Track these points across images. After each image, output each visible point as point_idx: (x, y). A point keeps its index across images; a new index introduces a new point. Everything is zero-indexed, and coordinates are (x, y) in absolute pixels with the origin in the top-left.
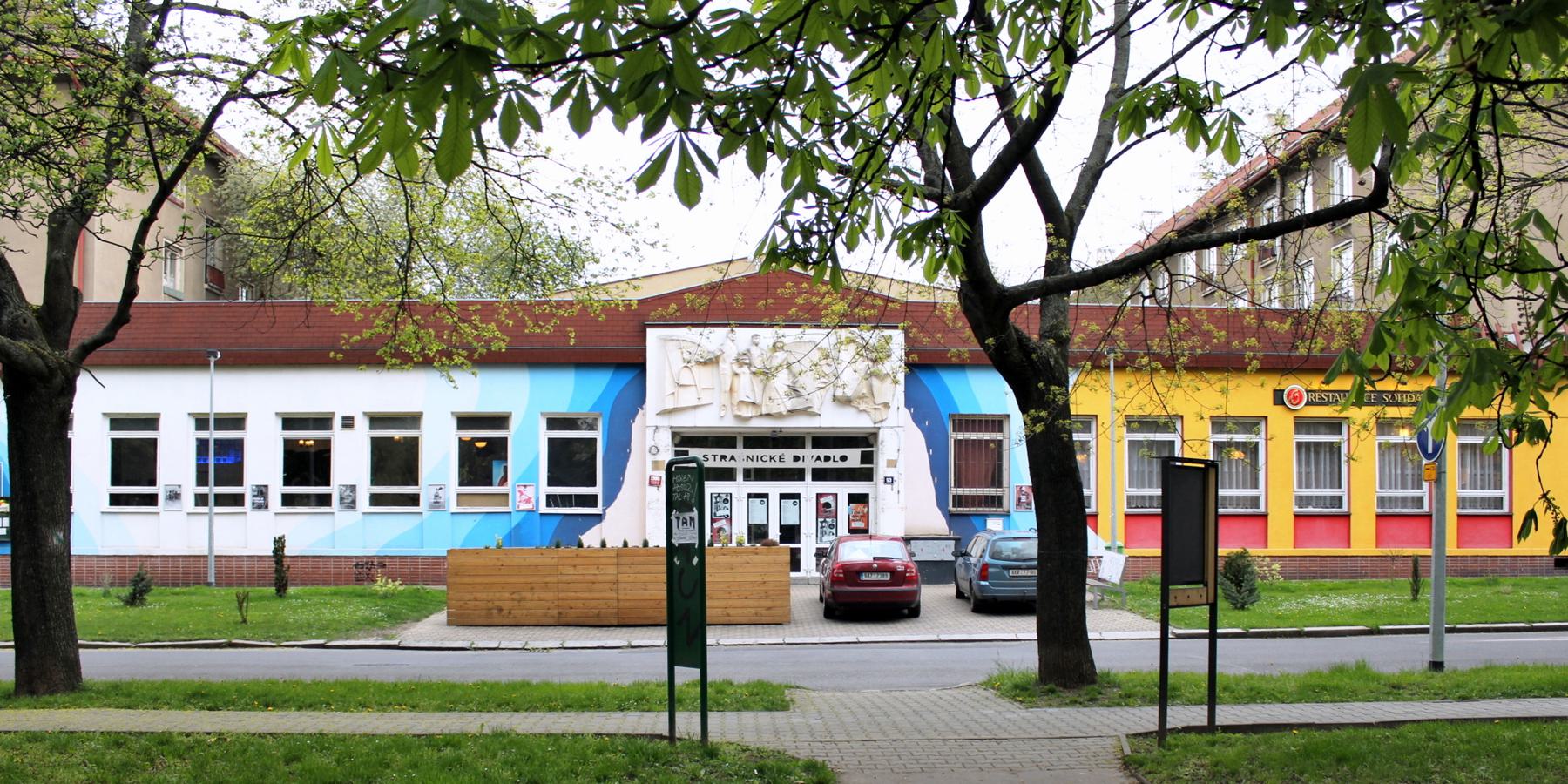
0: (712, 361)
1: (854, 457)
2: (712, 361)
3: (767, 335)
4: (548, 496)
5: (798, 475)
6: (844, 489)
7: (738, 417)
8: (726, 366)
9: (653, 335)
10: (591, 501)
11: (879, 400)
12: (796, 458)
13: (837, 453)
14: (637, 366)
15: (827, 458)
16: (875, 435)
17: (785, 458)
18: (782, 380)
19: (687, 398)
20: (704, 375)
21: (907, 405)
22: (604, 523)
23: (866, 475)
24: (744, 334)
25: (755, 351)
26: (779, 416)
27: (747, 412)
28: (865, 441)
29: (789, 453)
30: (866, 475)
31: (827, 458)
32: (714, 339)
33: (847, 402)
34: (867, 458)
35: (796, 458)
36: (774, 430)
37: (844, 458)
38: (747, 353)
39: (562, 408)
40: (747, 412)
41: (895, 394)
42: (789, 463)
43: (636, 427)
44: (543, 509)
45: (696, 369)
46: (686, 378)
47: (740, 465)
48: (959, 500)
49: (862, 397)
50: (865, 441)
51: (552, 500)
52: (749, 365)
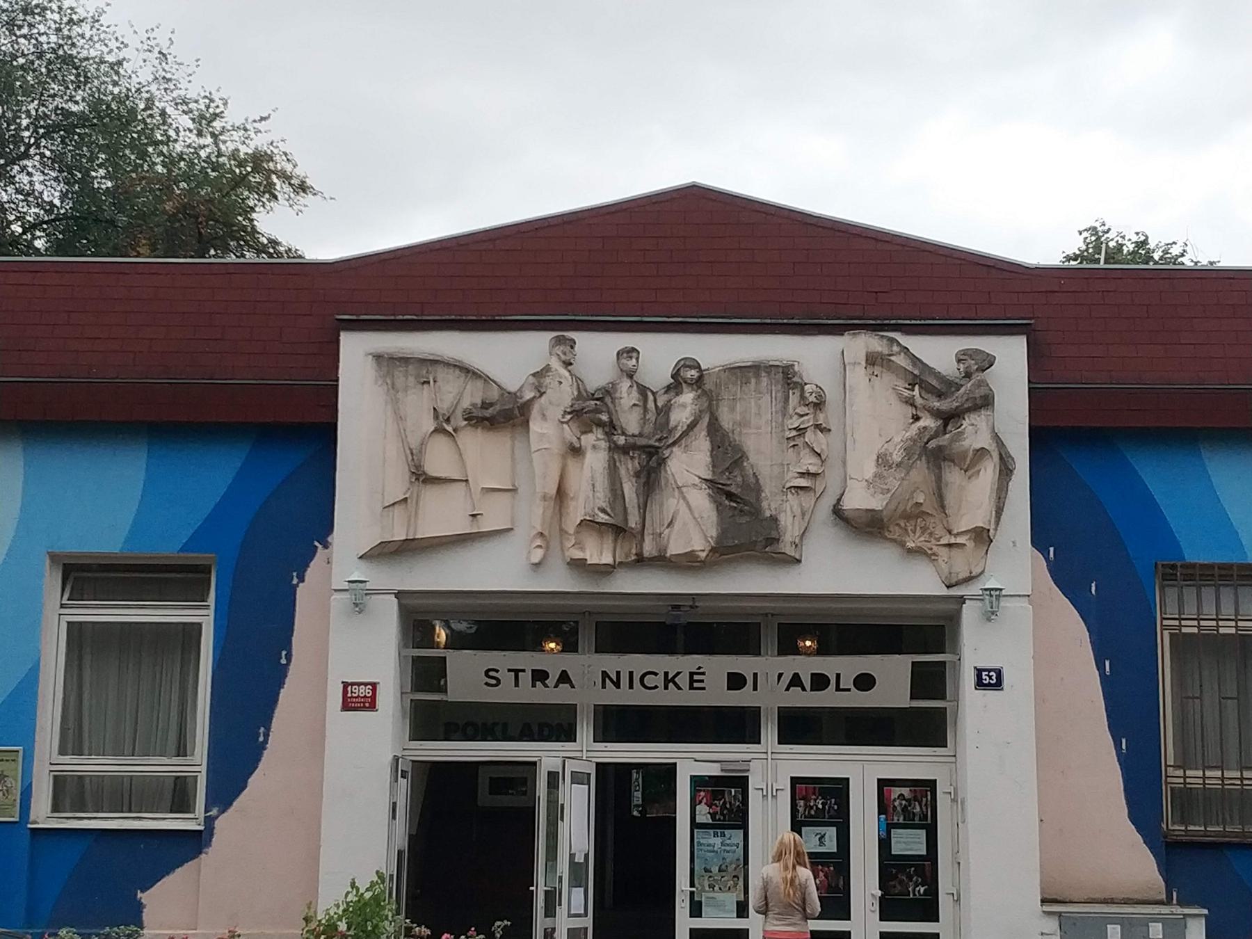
0: (504, 415)
1: (892, 681)
2: (504, 415)
3: (660, 353)
4: (59, 783)
5: (737, 725)
6: (863, 769)
7: (578, 565)
8: (547, 429)
9: (356, 352)
10: (178, 795)
11: (965, 524)
12: (736, 681)
13: (846, 666)
14: (310, 433)
15: (820, 682)
16: (954, 619)
17: (708, 679)
18: (689, 465)
19: (441, 514)
20: (484, 454)
21: (1039, 541)
22: (207, 859)
23: (927, 728)
24: (597, 352)
25: (627, 396)
26: (688, 564)
27: (598, 552)
28: (922, 635)
29: (716, 667)
30: (927, 728)
31: (820, 682)
32: (509, 357)
33: (867, 527)
34: (931, 681)
35: (736, 681)
36: (675, 602)
37: (865, 682)
38: (606, 394)
39: (107, 532)
40: (598, 552)
41: (996, 502)
42: (716, 695)
43: (304, 595)
44: (42, 815)
45: (474, 442)
46: (439, 460)
47: (587, 695)
48: (1186, 800)
49: (915, 515)
50: (922, 635)
51: (69, 793)
52: (611, 428)
